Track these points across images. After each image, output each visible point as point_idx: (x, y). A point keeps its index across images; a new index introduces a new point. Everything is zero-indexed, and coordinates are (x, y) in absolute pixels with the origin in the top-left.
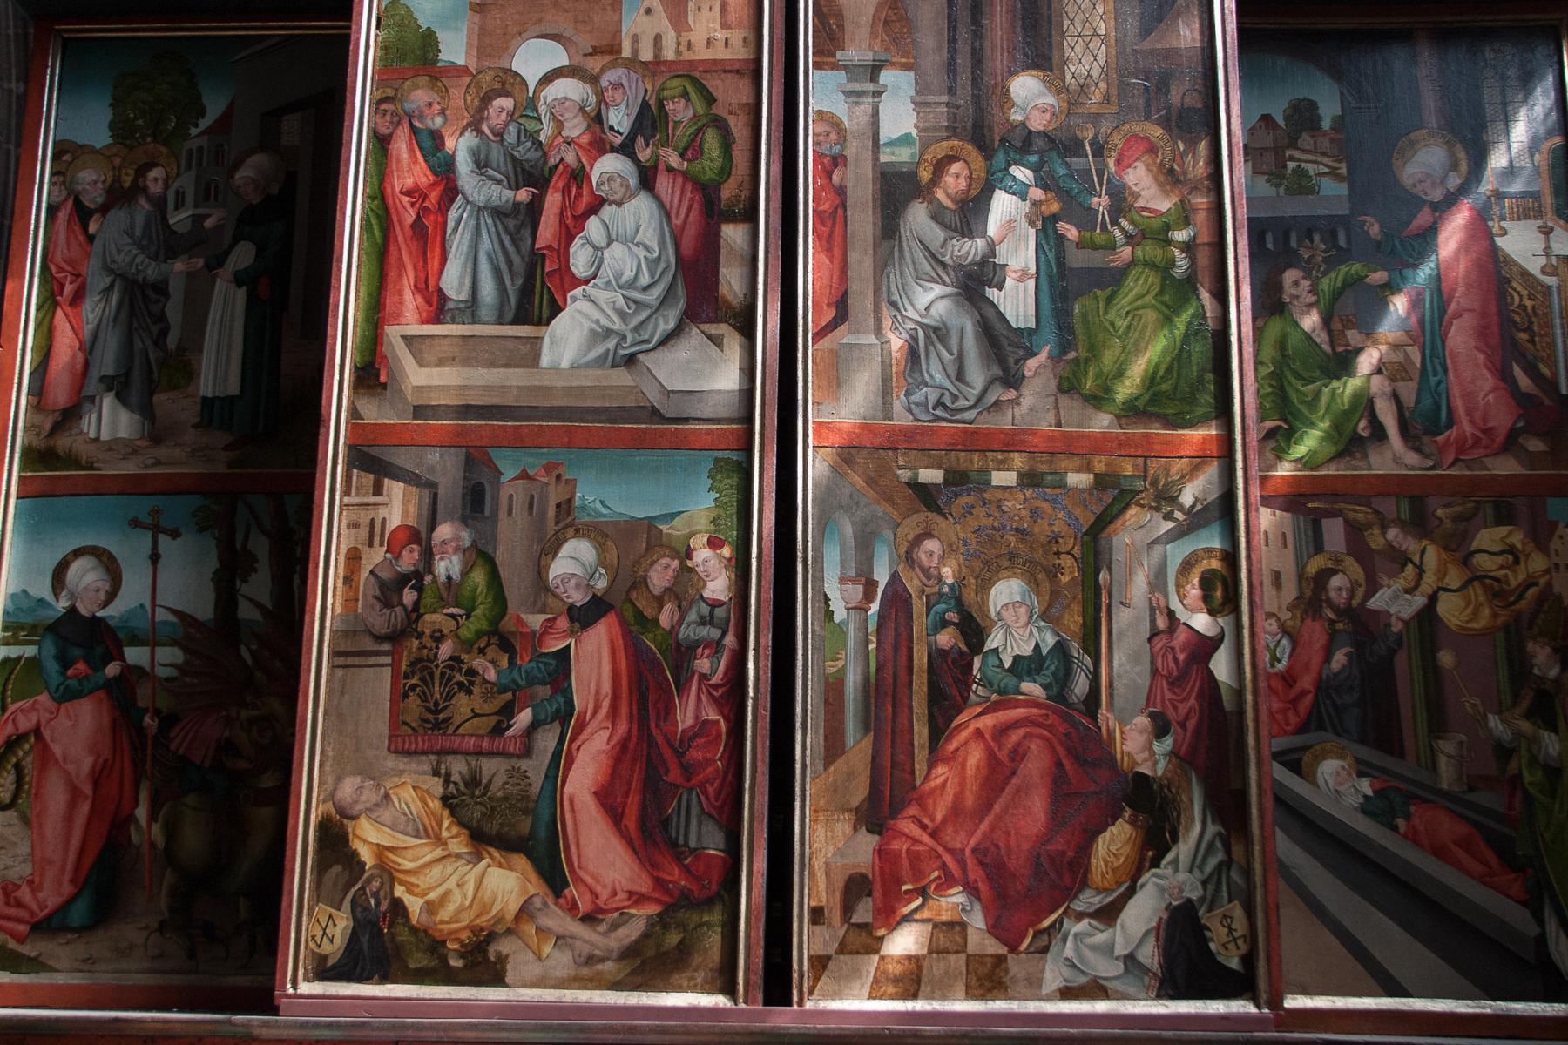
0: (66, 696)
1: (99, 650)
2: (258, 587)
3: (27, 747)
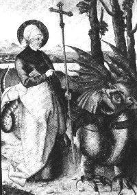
0: (29, 84)
1: (42, 65)
2: (109, 38)
3: (15, 106)
